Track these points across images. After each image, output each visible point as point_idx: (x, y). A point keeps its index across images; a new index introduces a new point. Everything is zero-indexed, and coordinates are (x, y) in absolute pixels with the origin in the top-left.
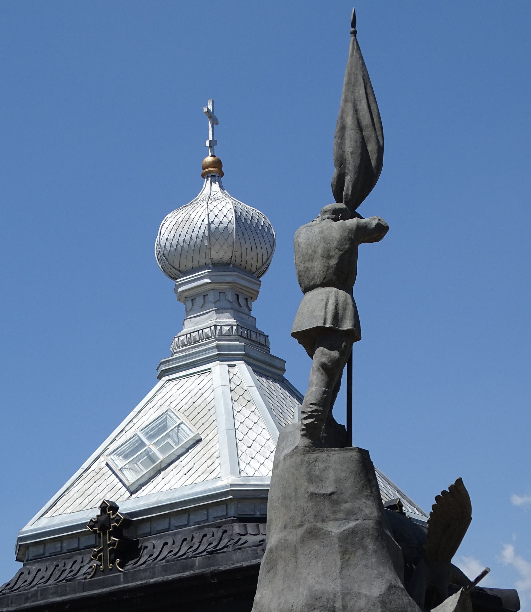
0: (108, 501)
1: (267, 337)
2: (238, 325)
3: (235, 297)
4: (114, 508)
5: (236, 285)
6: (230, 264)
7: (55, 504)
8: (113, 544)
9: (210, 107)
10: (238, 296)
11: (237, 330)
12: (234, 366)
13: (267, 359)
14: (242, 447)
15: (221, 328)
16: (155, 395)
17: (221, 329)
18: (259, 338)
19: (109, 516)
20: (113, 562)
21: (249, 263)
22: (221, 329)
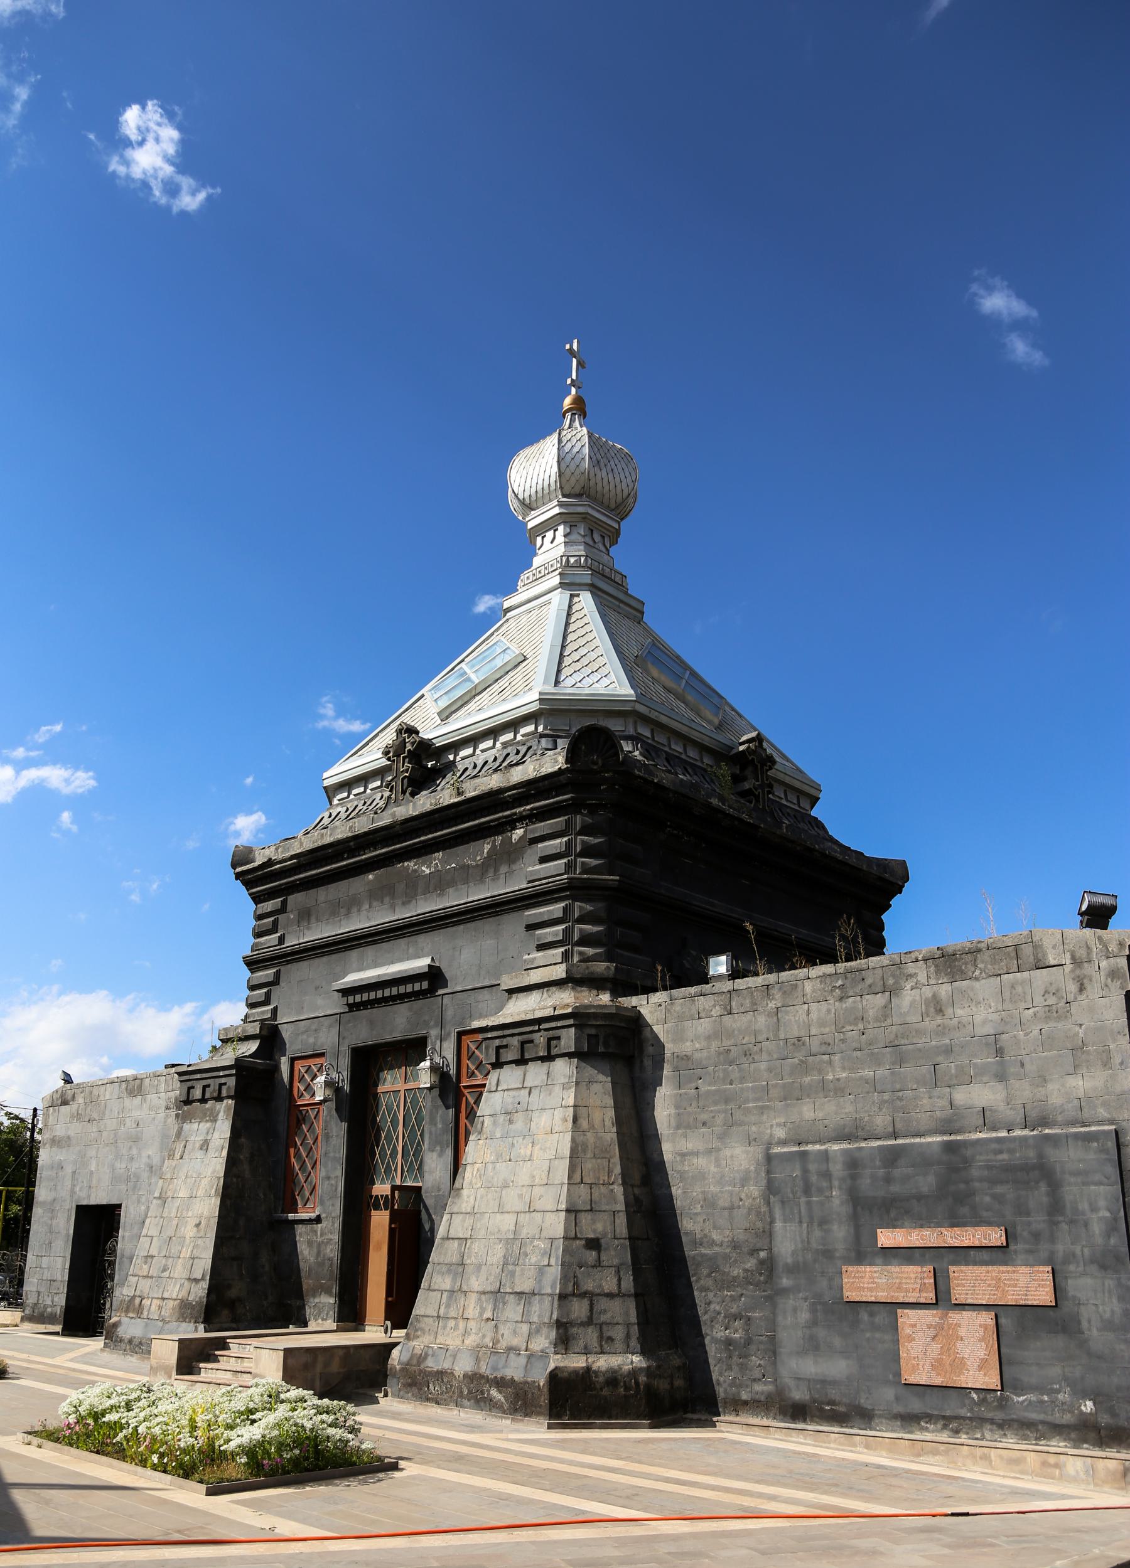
0: (405, 724)
1: (624, 578)
2: (587, 556)
3: (588, 533)
4: (412, 731)
5: (589, 517)
6: (583, 495)
7: (367, 744)
8: (407, 771)
9: (575, 347)
10: (592, 531)
11: (586, 560)
12: (578, 595)
13: (621, 596)
14: (567, 661)
15: (568, 559)
16: (492, 634)
17: (568, 561)
18: (613, 575)
19: (405, 739)
20: (404, 792)
21: (599, 488)
22: (568, 561)
